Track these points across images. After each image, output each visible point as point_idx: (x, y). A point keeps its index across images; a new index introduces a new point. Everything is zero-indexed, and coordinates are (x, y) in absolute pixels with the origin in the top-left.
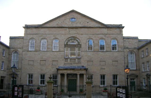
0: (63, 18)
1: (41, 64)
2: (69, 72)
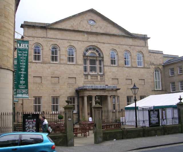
0: (79, 18)
2: (99, 93)
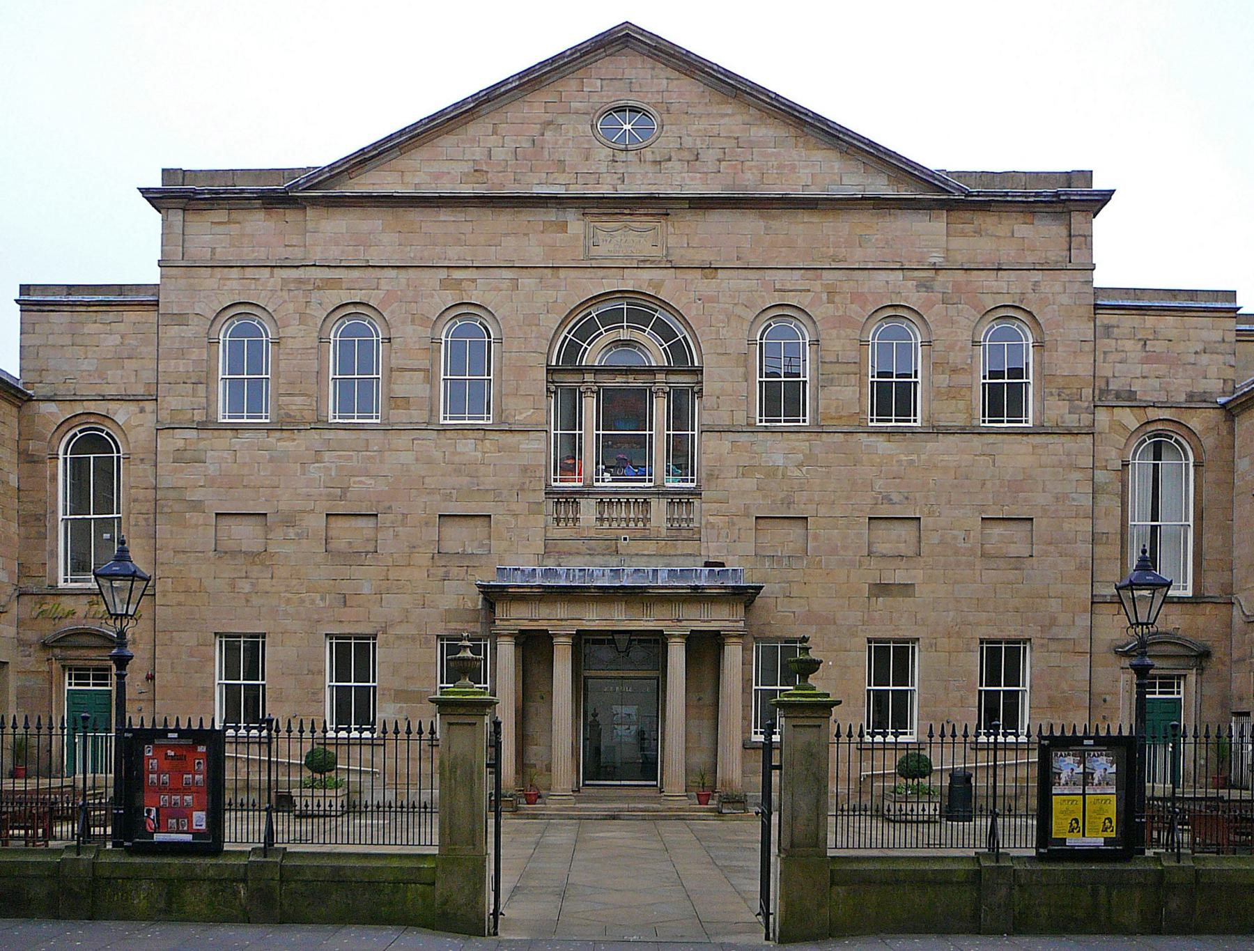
0: (534, 108)
1: (331, 546)
2: (594, 618)
